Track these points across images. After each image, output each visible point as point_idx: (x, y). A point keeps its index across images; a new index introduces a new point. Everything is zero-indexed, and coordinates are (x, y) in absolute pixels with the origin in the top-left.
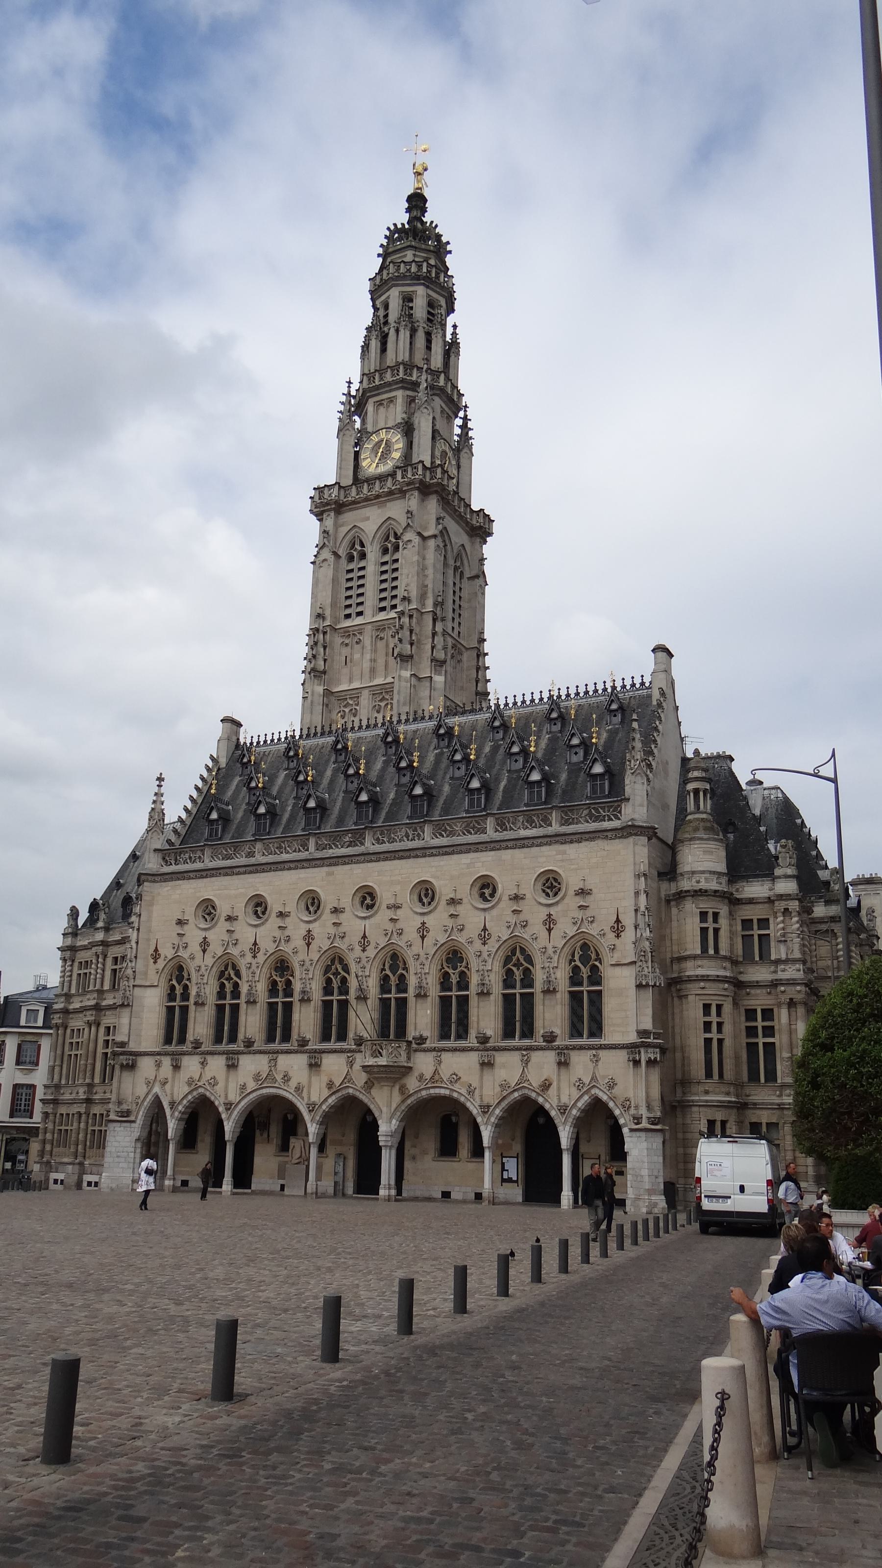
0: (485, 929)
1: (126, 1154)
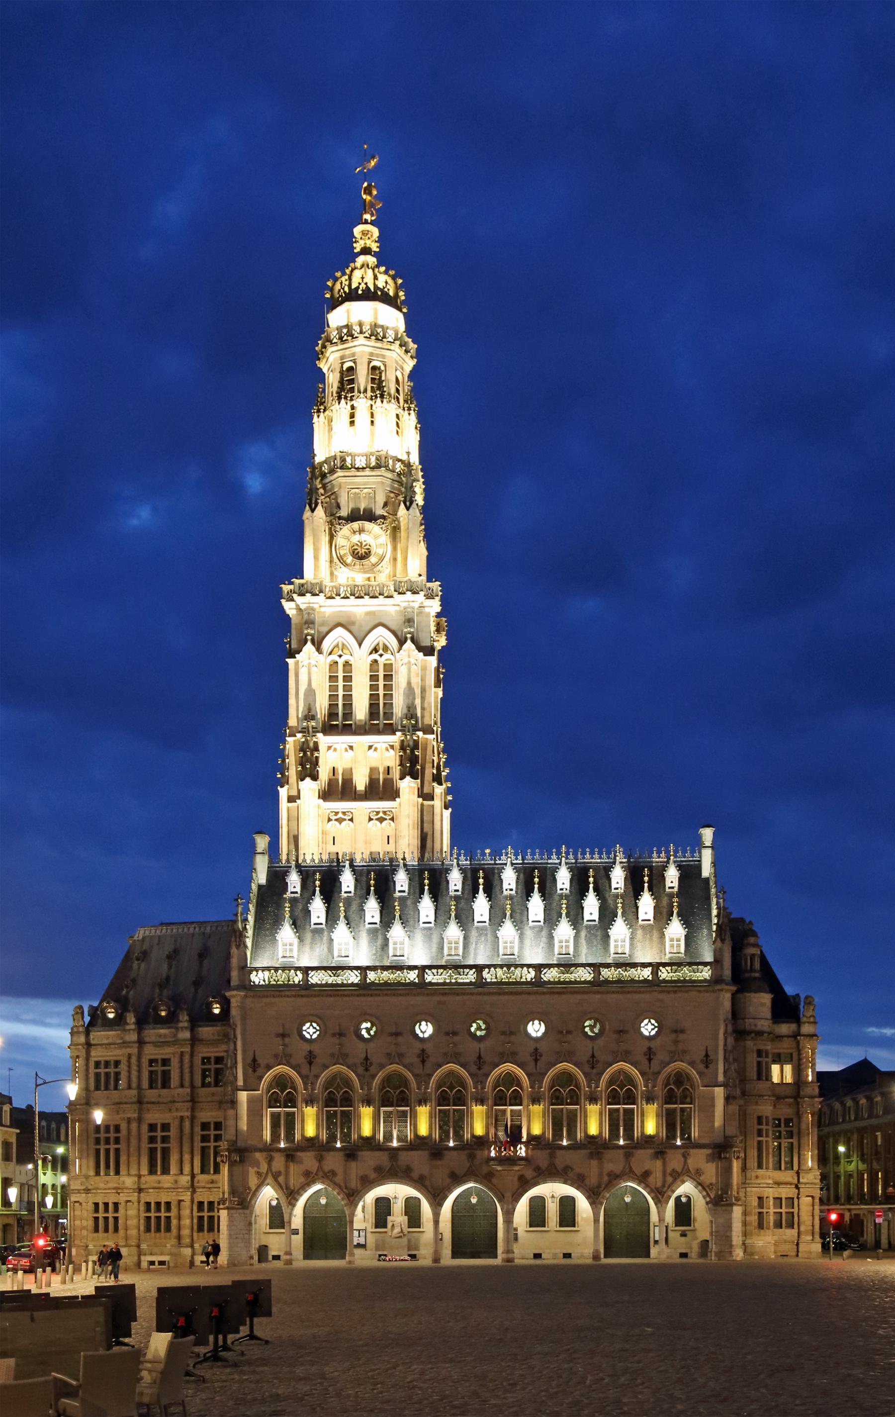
0: (593, 1056)
1: (241, 1236)
